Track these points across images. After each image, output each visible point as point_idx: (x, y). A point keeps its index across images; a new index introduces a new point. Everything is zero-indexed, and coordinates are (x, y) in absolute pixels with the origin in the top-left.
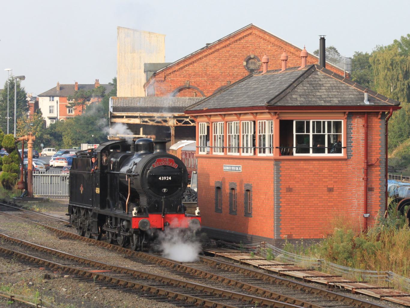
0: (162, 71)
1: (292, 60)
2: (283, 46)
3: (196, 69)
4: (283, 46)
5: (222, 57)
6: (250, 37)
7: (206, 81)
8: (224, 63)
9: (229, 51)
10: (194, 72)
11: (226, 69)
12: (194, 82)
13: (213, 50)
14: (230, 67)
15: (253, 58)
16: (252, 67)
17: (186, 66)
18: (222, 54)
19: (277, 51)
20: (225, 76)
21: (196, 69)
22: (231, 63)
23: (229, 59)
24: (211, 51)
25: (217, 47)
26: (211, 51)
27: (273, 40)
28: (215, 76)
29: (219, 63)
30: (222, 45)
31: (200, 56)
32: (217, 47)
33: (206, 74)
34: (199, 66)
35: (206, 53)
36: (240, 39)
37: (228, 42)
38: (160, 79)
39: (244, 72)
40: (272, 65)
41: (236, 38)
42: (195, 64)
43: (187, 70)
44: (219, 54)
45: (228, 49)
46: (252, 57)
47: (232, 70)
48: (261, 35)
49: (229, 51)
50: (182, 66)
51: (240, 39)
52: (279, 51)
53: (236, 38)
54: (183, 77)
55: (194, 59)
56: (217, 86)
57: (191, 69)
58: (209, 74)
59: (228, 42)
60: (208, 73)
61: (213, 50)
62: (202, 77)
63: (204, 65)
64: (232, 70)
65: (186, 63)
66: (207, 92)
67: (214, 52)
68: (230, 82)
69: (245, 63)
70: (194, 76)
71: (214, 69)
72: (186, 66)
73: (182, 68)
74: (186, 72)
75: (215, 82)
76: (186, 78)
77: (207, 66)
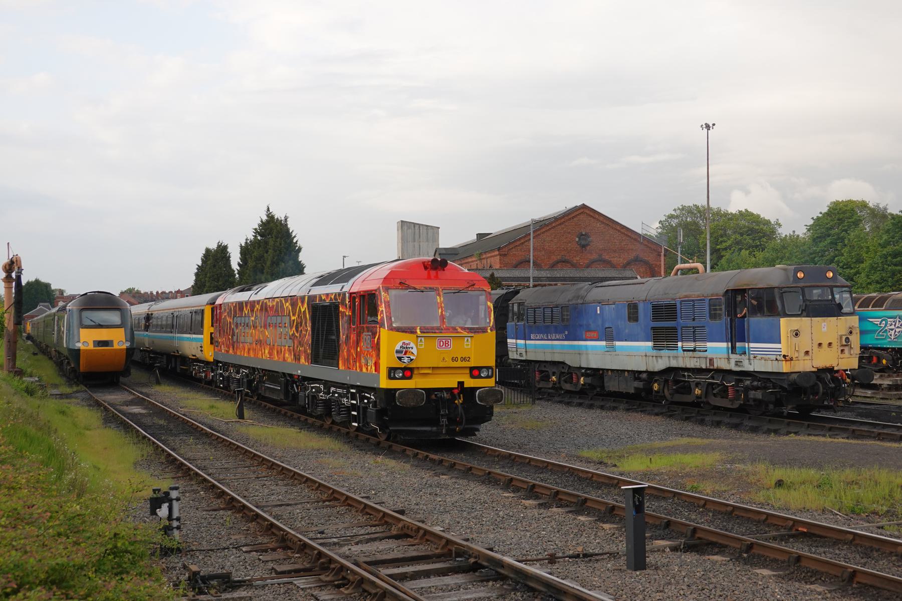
0: (506, 246)
2: (610, 224)
4: (610, 224)
6: (582, 217)
9: (563, 228)
15: (583, 235)
16: (583, 242)
19: (605, 228)
25: (554, 225)
27: (601, 219)
30: (557, 223)
33: (543, 249)
35: (544, 230)
36: (573, 218)
37: (563, 220)
38: (503, 253)
41: (570, 217)
45: (563, 226)
46: (584, 233)
48: (591, 214)
49: (563, 228)
50: (522, 241)
51: (573, 218)
52: (607, 228)
53: (570, 217)
59: (563, 220)
60: (545, 248)
67: (550, 229)
69: (577, 239)
73: (523, 243)
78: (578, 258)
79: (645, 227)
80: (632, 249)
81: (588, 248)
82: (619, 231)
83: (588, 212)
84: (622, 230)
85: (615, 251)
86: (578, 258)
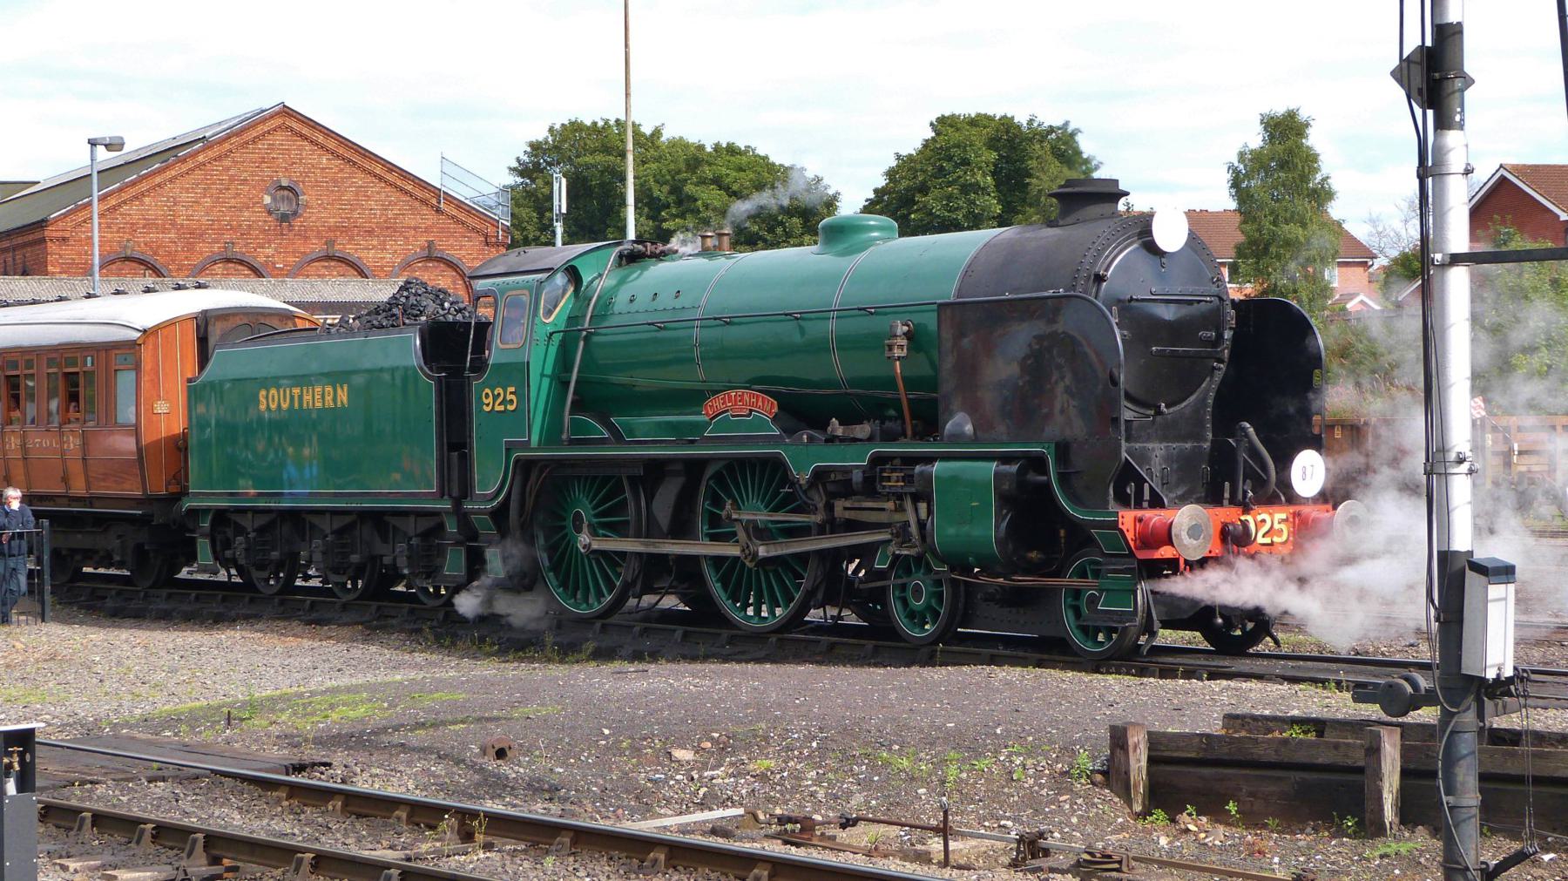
0: (65, 215)
1: (378, 193)
3: (148, 210)
5: (213, 184)
7: (175, 242)
8: (219, 198)
9: (228, 169)
10: (145, 219)
11: (223, 211)
12: (146, 244)
13: (190, 164)
14: (231, 207)
17: (125, 202)
18: (212, 175)
19: (341, 170)
20: (219, 229)
21: (148, 210)
22: (235, 198)
23: (229, 189)
24: (184, 168)
26: (184, 168)
28: (196, 229)
29: (205, 197)
31: (158, 180)
32: (201, 158)
33: (173, 224)
34: (156, 205)
35: (173, 173)
38: (60, 234)
39: (265, 221)
40: (333, 204)
42: (147, 200)
43: (126, 214)
44: (206, 175)
45: (227, 163)
47: (238, 216)
48: (305, 131)
54: (118, 232)
55: (144, 186)
56: (201, 253)
57: (138, 210)
58: (182, 225)
61: (190, 164)
62: (163, 233)
63: (168, 201)
64: (238, 216)
65: (125, 196)
66: (179, 269)
68: (233, 243)
69: (267, 200)
70: (143, 228)
71: (194, 211)
72: (125, 202)
74: (123, 219)
75: (194, 243)
76: (124, 233)
77: (175, 204)
78: (270, 251)
79: (448, 168)
80: (415, 228)
81: (297, 223)
82: (381, 179)
83: (295, 125)
84: (389, 177)
85: (370, 232)
86: (270, 251)
